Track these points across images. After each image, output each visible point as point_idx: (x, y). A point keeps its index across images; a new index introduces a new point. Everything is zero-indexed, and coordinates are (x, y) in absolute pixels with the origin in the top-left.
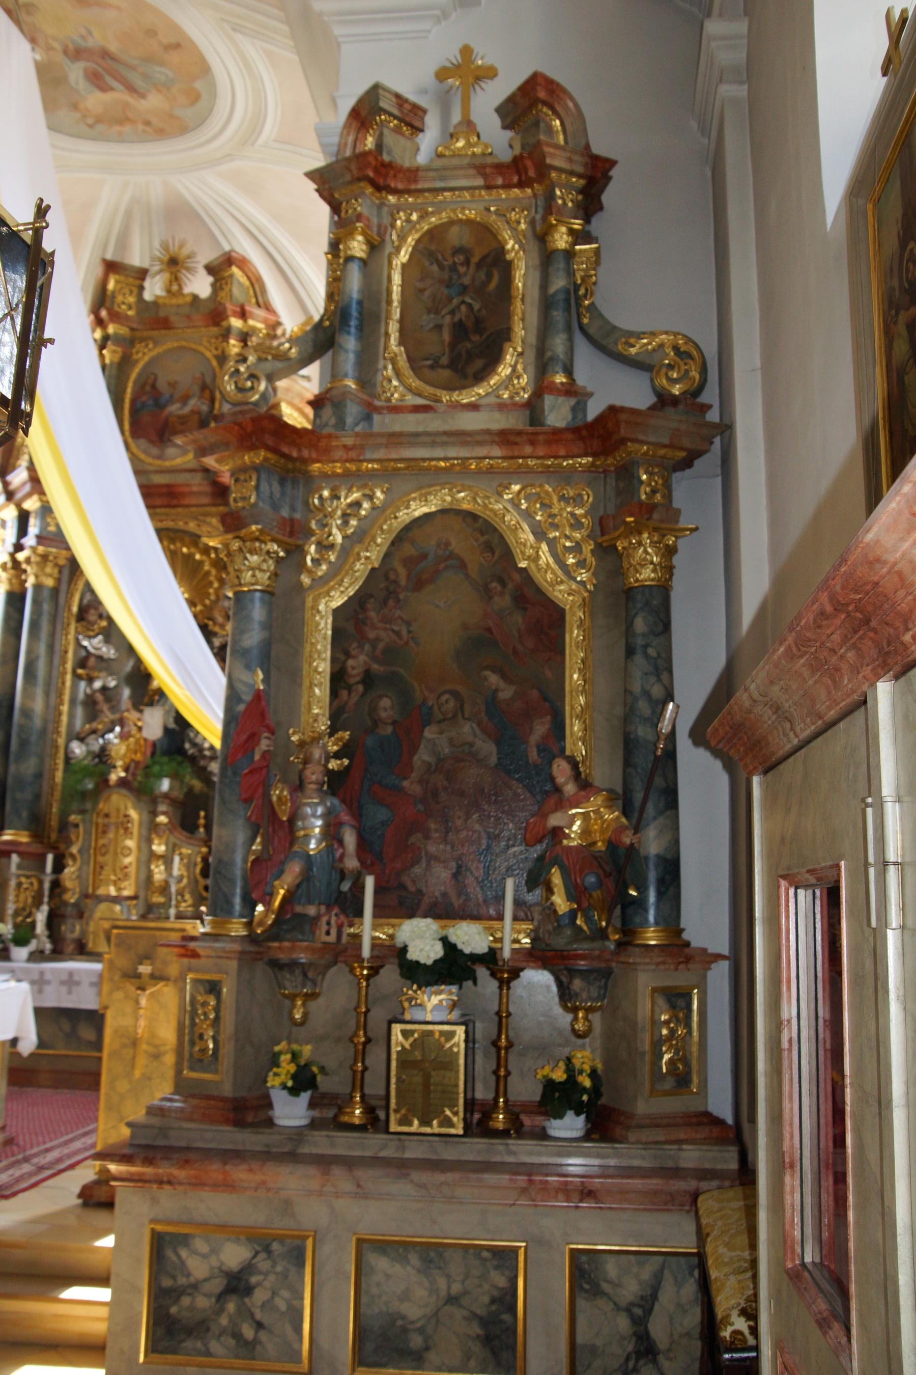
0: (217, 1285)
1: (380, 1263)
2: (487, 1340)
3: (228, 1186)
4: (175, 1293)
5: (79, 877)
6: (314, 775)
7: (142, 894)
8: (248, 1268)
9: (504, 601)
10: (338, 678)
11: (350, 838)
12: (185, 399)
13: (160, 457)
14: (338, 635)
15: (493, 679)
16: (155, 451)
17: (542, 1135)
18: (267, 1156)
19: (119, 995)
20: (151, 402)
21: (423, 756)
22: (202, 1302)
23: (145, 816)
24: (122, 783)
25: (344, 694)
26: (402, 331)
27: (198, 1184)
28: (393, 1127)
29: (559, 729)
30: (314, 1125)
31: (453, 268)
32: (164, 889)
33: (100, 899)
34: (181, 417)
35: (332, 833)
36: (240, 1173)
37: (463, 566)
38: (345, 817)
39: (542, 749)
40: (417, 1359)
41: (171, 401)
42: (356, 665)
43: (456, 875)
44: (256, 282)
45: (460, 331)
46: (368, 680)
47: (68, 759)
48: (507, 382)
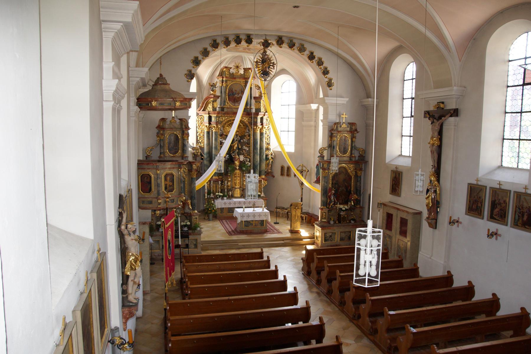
0: (329, 237)
3: (330, 229)
4: (326, 238)
8: (332, 235)
9: (347, 176)
10: (332, 183)
11: (335, 199)
12: (238, 94)
13: (234, 105)
14: (333, 180)
15: (346, 183)
16: (233, 104)
17: (351, 222)
19: (293, 211)
20: (232, 94)
21: (340, 190)
22: (328, 238)
23: (242, 174)
27: (328, 229)
29: (351, 188)
33: (236, 188)
34: (237, 97)
35: (334, 198)
37: (343, 172)
38: (334, 197)
39: (350, 190)
41: (236, 94)
42: (334, 182)
46: (335, 183)
48: (348, 154)
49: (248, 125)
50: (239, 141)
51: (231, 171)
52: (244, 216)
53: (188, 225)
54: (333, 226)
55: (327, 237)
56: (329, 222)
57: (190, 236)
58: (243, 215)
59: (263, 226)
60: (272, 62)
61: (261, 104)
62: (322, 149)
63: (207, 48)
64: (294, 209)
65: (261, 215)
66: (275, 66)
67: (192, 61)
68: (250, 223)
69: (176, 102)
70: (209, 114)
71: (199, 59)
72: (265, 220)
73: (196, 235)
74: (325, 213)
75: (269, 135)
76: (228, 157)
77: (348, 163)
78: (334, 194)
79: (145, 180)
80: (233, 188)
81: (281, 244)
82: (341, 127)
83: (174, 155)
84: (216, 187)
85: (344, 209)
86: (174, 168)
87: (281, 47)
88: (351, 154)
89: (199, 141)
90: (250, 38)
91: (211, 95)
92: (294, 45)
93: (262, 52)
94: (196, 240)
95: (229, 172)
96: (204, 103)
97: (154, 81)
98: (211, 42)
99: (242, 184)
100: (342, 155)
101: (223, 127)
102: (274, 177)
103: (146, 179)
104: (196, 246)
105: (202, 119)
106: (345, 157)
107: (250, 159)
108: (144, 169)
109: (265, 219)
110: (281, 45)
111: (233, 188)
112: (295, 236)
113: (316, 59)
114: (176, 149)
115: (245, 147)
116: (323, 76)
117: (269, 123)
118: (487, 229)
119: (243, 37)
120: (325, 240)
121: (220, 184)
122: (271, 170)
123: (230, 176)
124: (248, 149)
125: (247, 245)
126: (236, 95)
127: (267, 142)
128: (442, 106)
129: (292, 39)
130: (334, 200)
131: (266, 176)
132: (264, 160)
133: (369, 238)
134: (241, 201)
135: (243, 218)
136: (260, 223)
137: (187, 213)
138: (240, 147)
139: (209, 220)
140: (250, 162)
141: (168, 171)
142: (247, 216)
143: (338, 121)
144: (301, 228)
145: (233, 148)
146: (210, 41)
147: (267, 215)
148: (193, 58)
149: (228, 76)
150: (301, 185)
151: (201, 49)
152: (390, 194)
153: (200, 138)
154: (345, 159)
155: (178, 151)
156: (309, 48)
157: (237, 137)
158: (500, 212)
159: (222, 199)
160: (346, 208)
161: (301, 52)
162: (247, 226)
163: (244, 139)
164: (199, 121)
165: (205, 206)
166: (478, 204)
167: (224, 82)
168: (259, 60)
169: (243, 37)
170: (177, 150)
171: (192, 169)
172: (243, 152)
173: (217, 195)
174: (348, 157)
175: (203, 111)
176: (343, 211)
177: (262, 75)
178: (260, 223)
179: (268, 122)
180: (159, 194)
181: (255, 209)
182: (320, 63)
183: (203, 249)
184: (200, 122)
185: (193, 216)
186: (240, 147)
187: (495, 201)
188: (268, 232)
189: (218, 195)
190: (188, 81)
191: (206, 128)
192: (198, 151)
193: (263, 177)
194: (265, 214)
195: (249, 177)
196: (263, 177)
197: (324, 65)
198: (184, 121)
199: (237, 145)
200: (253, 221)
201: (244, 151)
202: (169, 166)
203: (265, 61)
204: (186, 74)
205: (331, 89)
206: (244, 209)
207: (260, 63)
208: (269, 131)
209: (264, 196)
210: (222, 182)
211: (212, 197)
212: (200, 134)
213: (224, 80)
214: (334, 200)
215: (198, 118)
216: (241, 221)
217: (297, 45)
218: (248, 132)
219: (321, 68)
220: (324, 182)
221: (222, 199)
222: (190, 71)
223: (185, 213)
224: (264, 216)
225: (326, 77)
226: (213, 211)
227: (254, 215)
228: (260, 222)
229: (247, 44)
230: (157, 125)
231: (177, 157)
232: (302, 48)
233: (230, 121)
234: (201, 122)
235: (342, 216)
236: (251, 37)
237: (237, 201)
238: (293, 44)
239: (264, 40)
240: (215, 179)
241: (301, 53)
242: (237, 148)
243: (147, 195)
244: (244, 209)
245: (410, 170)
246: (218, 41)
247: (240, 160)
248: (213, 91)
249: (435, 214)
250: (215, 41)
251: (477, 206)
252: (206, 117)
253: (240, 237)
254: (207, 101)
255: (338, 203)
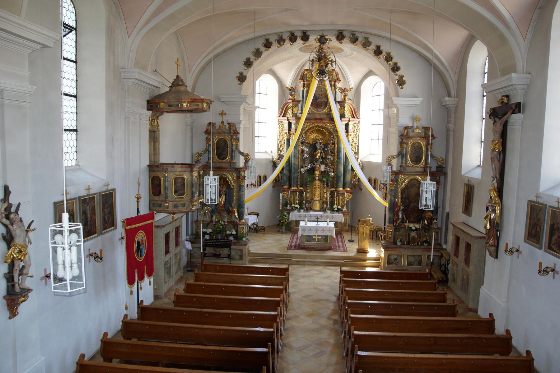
0: (394, 259)
1: (409, 257)
2: (419, 263)
3: (395, 250)
4: (390, 260)
5: (310, 196)
6: (401, 210)
7: (322, 199)
8: (397, 258)
10: (402, 198)
11: (404, 216)
13: (317, 111)
14: (402, 193)
16: (316, 109)
17: (423, 245)
18: (397, 248)
19: (361, 227)
21: (411, 206)
22: (392, 261)
23: (322, 185)
24: (318, 180)
25: (402, 199)
26: (410, 157)
27: (392, 250)
28: (410, 245)
30: (401, 244)
31: (416, 149)
32: (326, 198)
34: (321, 102)
35: (402, 215)
36: (397, 249)
37: (416, 185)
38: (403, 214)
40: (412, 265)
42: (404, 196)
43: (414, 219)
44: (337, 74)
45: (417, 157)
46: (405, 198)
47: (301, 173)
48: (422, 164)
49: (333, 132)
50: (324, 149)
51: (310, 181)
52: (306, 230)
53: (233, 234)
54: (400, 247)
55: (392, 260)
56: (395, 243)
57: (233, 247)
58: (304, 228)
59: (328, 242)
60: (330, 59)
61: (346, 109)
62: (390, 158)
63: (259, 48)
64: (362, 226)
65: (305, 229)
66: (334, 64)
67: (243, 63)
68: (312, 237)
69: (183, 103)
70: (288, 120)
71: (252, 60)
72: (330, 236)
73: (242, 245)
74: (390, 231)
75: (356, 144)
76: (310, 167)
77: (421, 174)
78: (403, 210)
79: (155, 182)
80: (312, 200)
81: (340, 264)
82: (413, 132)
83: (223, 161)
84: (294, 198)
85: (414, 228)
86: (185, 171)
87: (341, 43)
88: (426, 163)
89: (280, 149)
90: (306, 35)
91: (289, 99)
92: (357, 39)
93: (317, 50)
94: (241, 251)
95: (308, 183)
96: (283, 109)
97: (172, 83)
98: (263, 42)
99: (322, 196)
100: (413, 165)
101: (306, 134)
102: (361, 190)
103: (157, 182)
104: (241, 257)
105: (283, 125)
106: (418, 167)
107: (334, 169)
108: (154, 171)
109: (329, 235)
110: (341, 40)
111: (312, 200)
112: (361, 256)
113: (384, 53)
114: (225, 155)
115: (329, 157)
116: (392, 73)
117: (357, 130)
118: (539, 263)
119: (299, 34)
120: (389, 263)
121: (297, 195)
122: (358, 182)
123: (309, 187)
124: (332, 159)
125: (301, 261)
126: (319, 100)
127: (355, 151)
128: (505, 100)
129: (354, 32)
130: (403, 217)
131: (351, 189)
132: (350, 171)
133: (66, 233)
134: (318, 215)
135: (304, 232)
136: (324, 239)
137: (234, 222)
138: (324, 156)
139: (282, 233)
140: (333, 172)
141: (178, 175)
142: (309, 230)
143: (410, 125)
144: (370, 246)
145: (316, 157)
146: (263, 41)
147: (331, 231)
148: (245, 60)
149: (310, 79)
150: (385, 199)
151: (254, 50)
152: (463, 213)
153: (281, 145)
154: (418, 169)
155: (227, 157)
156: (375, 41)
157: (320, 145)
158: (558, 240)
159: (299, 211)
160: (416, 228)
161: (365, 46)
162: (309, 241)
163: (329, 147)
164: (280, 128)
165: (278, 217)
166: (537, 228)
167: (306, 86)
168: (315, 58)
169: (299, 34)
170: (225, 156)
171: (240, 175)
172: (326, 161)
173: (293, 207)
174: (421, 167)
175: (283, 116)
176: (413, 231)
177: (319, 75)
178: (324, 239)
179: (356, 128)
180: (166, 197)
181: (319, 223)
182: (388, 58)
183: (251, 262)
184: (281, 129)
185: (239, 226)
186: (324, 156)
187: (554, 224)
188: (332, 249)
189: (294, 207)
190: (240, 84)
191: (286, 135)
192: (247, 157)
193: (348, 189)
194: (330, 229)
195: (208, 179)
196: (348, 189)
197: (394, 60)
198: (233, 126)
199: (320, 154)
200: (315, 236)
201: (328, 161)
202: (180, 169)
203: (322, 59)
204: (237, 77)
205: (402, 88)
206: (306, 223)
207: (316, 61)
208: (357, 139)
209: (347, 210)
210: (301, 193)
211: (288, 208)
212: (281, 142)
213: (306, 84)
214: (403, 217)
215: (279, 124)
216: (302, 235)
217: (360, 39)
218: (332, 140)
219: (389, 65)
220: (391, 195)
221: (299, 211)
222: (241, 74)
223: (232, 222)
224: (328, 231)
225: (396, 75)
226: (286, 223)
227: (317, 229)
228: (324, 237)
229: (303, 42)
230: (205, 130)
231: (226, 163)
232: (366, 42)
233: (312, 128)
234: (282, 129)
235: (411, 237)
236: (308, 33)
237: (313, 215)
238: (356, 39)
239: (320, 36)
240: (293, 189)
241: (365, 48)
242: (320, 157)
243: (157, 198)
244: (306, 223)
245: (480, 182)
246: (270, 41)
247: (321, 170)
248: (291, 95)
249: (495, 239)
250: (267, 40)
251: (536, 231)
252: (286, 123)
253: (297, 252)
254: (286, 106)
255: (407, 221)
